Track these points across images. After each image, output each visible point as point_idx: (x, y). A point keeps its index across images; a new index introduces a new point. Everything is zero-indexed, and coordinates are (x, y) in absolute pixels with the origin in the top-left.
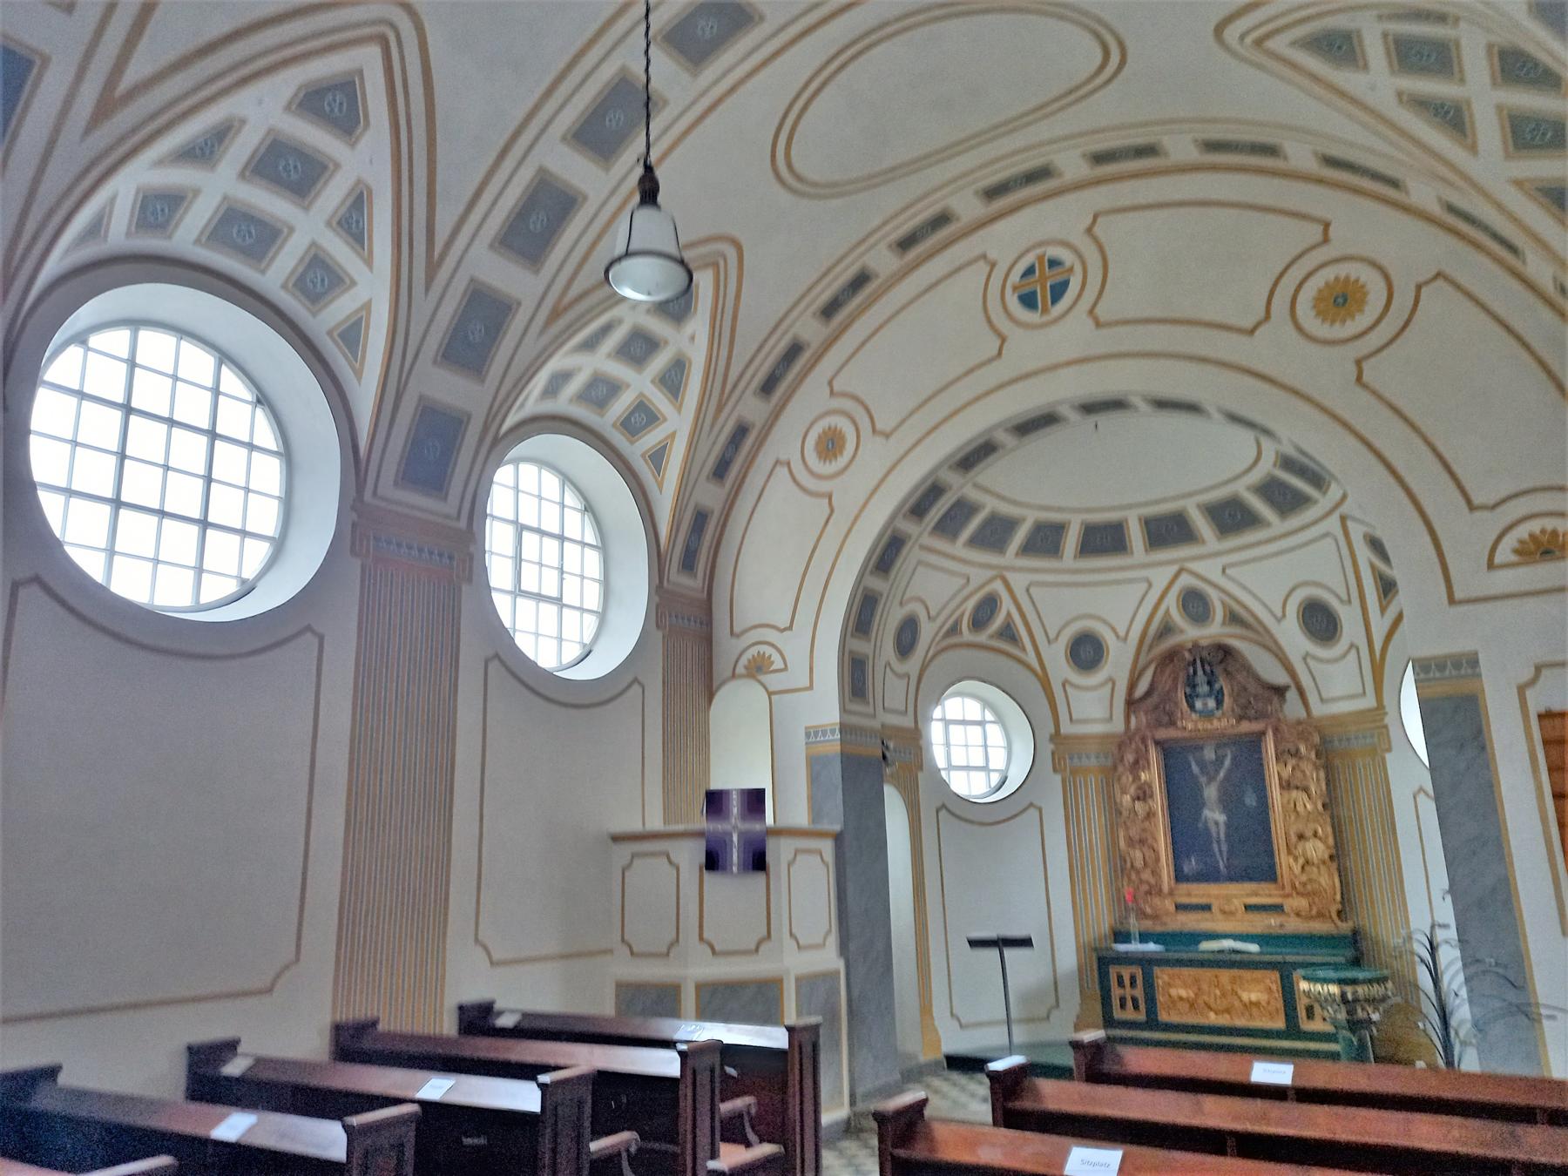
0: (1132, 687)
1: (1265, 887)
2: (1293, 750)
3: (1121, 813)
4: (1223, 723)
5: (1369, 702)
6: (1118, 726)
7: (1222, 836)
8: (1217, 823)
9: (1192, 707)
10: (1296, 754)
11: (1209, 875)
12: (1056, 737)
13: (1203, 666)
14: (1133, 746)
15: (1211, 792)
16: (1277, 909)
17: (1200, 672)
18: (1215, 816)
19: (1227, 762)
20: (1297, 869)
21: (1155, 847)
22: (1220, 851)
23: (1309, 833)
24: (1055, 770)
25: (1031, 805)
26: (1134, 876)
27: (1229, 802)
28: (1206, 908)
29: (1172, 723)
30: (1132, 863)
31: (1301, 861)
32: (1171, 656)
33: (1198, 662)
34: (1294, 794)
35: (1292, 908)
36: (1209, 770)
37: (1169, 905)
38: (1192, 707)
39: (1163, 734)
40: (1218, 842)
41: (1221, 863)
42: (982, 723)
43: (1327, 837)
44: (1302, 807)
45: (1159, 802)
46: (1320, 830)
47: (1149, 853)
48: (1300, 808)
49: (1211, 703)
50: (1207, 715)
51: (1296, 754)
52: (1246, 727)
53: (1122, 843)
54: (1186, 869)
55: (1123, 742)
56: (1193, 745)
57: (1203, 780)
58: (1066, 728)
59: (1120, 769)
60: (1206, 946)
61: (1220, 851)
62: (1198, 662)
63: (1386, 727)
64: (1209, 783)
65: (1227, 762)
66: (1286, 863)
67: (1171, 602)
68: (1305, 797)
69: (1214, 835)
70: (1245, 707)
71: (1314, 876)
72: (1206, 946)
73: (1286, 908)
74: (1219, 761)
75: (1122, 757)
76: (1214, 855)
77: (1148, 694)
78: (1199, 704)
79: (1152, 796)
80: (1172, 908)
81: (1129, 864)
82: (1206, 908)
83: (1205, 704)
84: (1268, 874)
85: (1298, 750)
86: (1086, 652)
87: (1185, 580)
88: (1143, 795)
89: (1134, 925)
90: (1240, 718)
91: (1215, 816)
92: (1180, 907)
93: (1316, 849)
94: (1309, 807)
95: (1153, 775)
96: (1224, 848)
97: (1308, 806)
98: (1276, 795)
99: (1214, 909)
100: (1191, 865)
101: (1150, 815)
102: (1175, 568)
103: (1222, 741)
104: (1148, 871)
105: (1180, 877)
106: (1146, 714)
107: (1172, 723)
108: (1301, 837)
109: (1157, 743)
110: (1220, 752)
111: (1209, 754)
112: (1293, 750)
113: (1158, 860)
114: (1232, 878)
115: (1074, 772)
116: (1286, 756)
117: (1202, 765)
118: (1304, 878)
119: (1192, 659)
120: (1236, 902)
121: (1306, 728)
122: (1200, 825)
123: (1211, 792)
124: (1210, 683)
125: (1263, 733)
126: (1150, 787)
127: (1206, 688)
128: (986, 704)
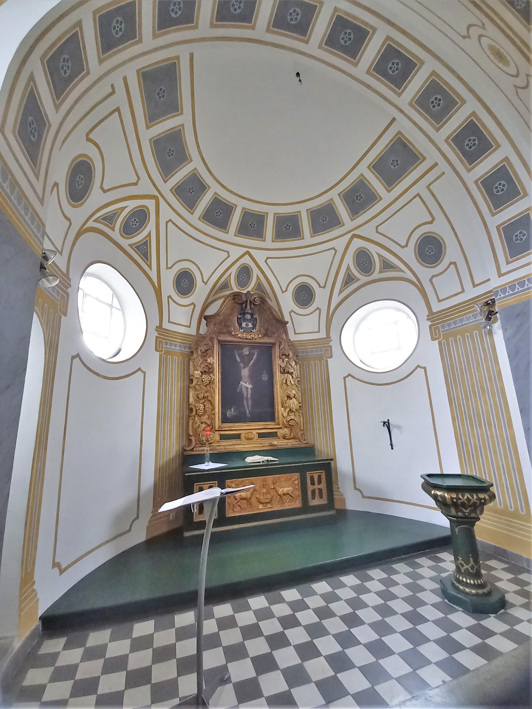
0: (204, 310)
1: (271, 425)
2: (287, 354)
3: (191, 381)
4: (256, 336)
5: (323, 334)
6: (193, 331)
7: (249, 396)
8: (247, 388)
9: (240, 325)
10: (287, 356)
11: (240, 418)
12: (159, 328)
13: (250, 306)
14: (205, 342)
15: (245, 372)
16: (274, 435)
17: (248, 307)
18: (246, 385)
19: (255, 357)
20: (285, 414)
21: (212, 401)
22: (248, 405)
23: (292, 396)
24: (156, 350)
25: (139, 369)
26: (196, 419)
27: (254, 378)
28: (238, 437)
29: (230, 333)
30: (196, 412)
31: (288, 410)
32: (236, 296)
33: (249, 302)
34: (286, 375)
35: (281, 434)
36: (246, 360)
37: (216, 436)
38: (240, 325)
39: (222, 338)
40: (247, 399)
41: (248, 412)
42: (111, 306)
43: (299, 398)
44: (289, 382)
45: (217, 376)
46: (296, 395)
47: (208, 405)
48: (288, 383)
49: (250, 325)
50: (248, 331)
51: (287, 356)
52: (266, 340)
53: (191, 400)
54: (228, 414)
55: (199, 339)
56: (239, 347)
57: (242, 365)
58: (166, 325)
59: (195, 355)
60: (249, 460)
61: (248, 405)
62: (249, 302)
63: (331, 347)
64: (244, 367)
65: (255, 357)
66: (280, 411)
67: (234, 271)
68: (291, 376)
69: (245, 395)
70: (267, 330)
71: (293, 418)
72: (249, 460)
73: (279, 434)
74: (251, 356)
75: (197, 348)
76: (244, 406)
77: (217, 314)
78: (244, 325)
79: (212, 372)
80: (218, 438)
81: (194, 413)
82: (238, 437)
83: (247, 325)
84: (272, 417)
85: (289, 355)
86: (185, 283)
87: (246, 260)
88: (208, 371)
89: (206, 450)
90: (265, 335)
91: (246, 385)
92: (223, 437)
93: (294, 403)
94: (293, 382)
95: (215, 360)
96: (250, 403)
97: (292, 382)
98: (278, 377)
99: (242, 436)
100: (231, 413)
101: (211, 382)
102: (246, 250)
103: (253, 346)
104: (206, 416)
105: (225, 419)
106: (215, 325)
107: (230, 333)
108: (289, 397)
109: (219, 341)
110: (252, 351)
111: (246, 351)
112: (287, 354)
113: (213, 409)
114: (253, 419)
115: (167, 353)
116: (284, 357)
117: (241, 356)
118: (289, 418)
119: (245, 300)
120: (254, 432)
121: (292, 345)
122: (238, 390)
123: (245, 372)
124: (252, 315)
125: (274, 344)
126: (213, 367)
127: (248, 317)
128: (115, 294)
